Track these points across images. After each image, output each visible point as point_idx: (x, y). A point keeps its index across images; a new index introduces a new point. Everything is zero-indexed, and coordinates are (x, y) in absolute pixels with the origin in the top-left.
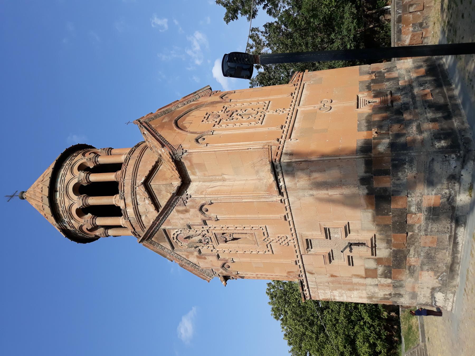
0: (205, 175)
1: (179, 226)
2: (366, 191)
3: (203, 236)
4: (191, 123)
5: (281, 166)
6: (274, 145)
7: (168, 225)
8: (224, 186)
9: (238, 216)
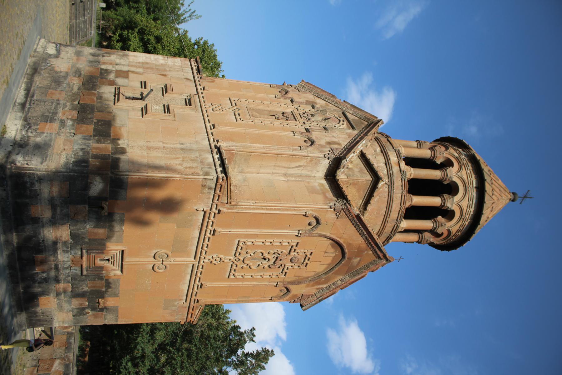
2: (120, 142)
3: (309, 119)
4: (325, 252)
5: (217, 172)
7: (350, 133)
8: (285, 167)
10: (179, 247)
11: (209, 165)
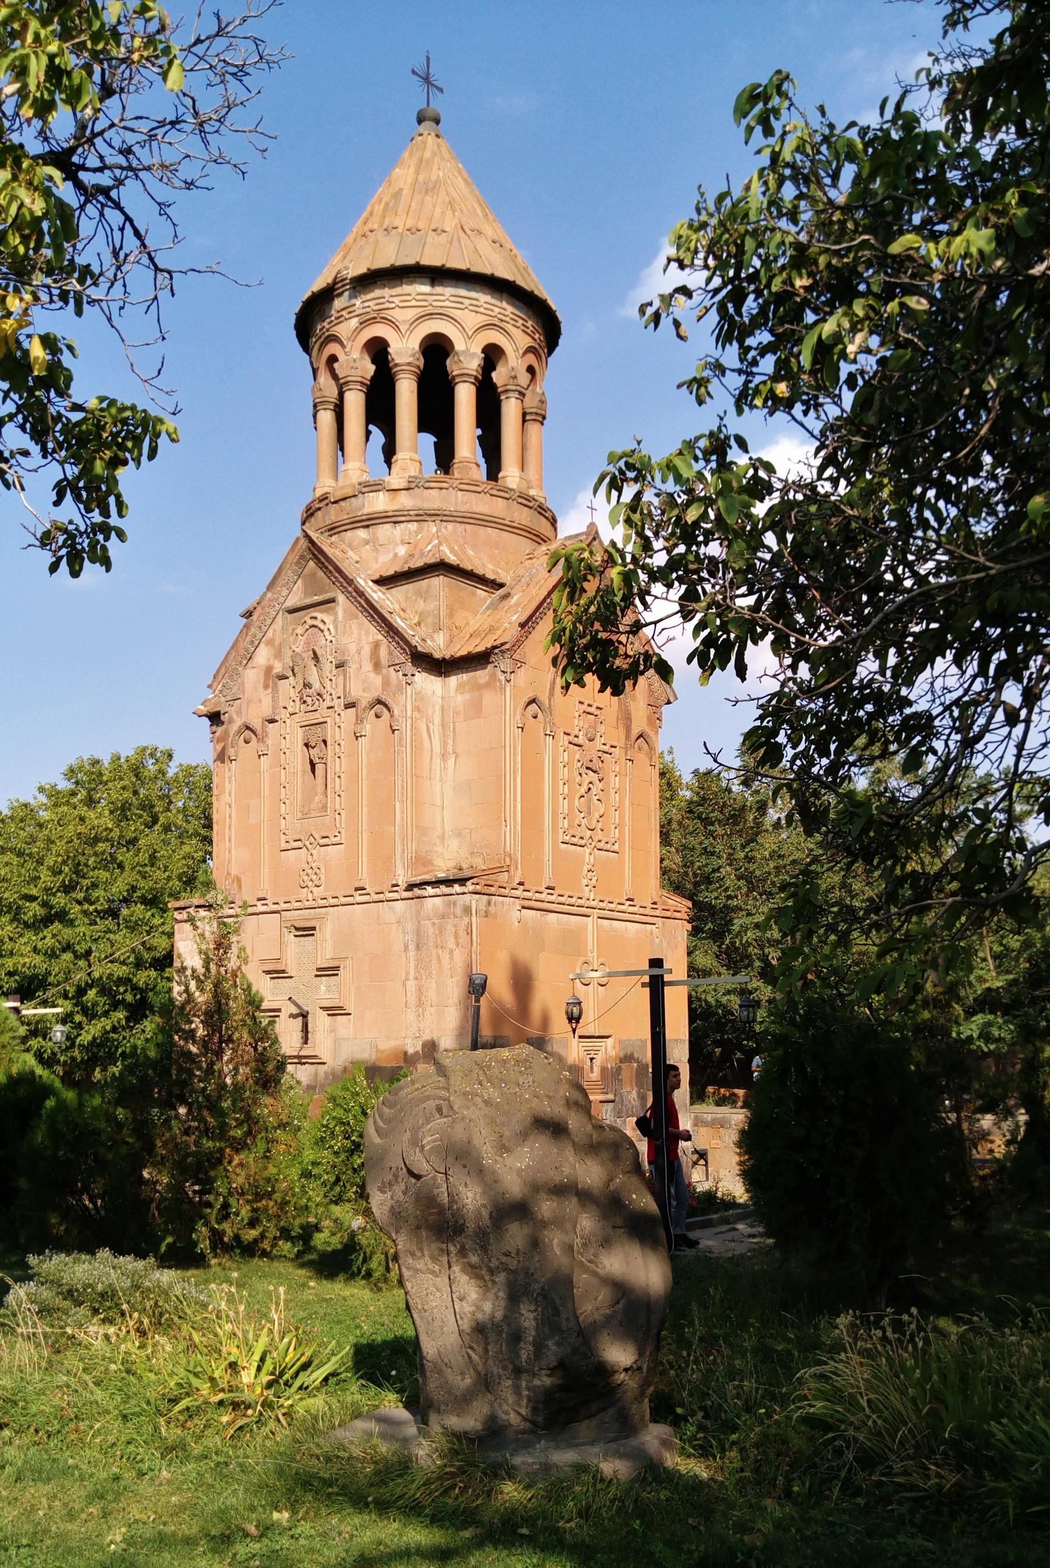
0: (456, 713)
1: (345, 640)
2: (411, 1051)
6: (510, 877)
7: (345, 611)
9: (365, 787)
10: (573, 944)
11: (448, 905)
